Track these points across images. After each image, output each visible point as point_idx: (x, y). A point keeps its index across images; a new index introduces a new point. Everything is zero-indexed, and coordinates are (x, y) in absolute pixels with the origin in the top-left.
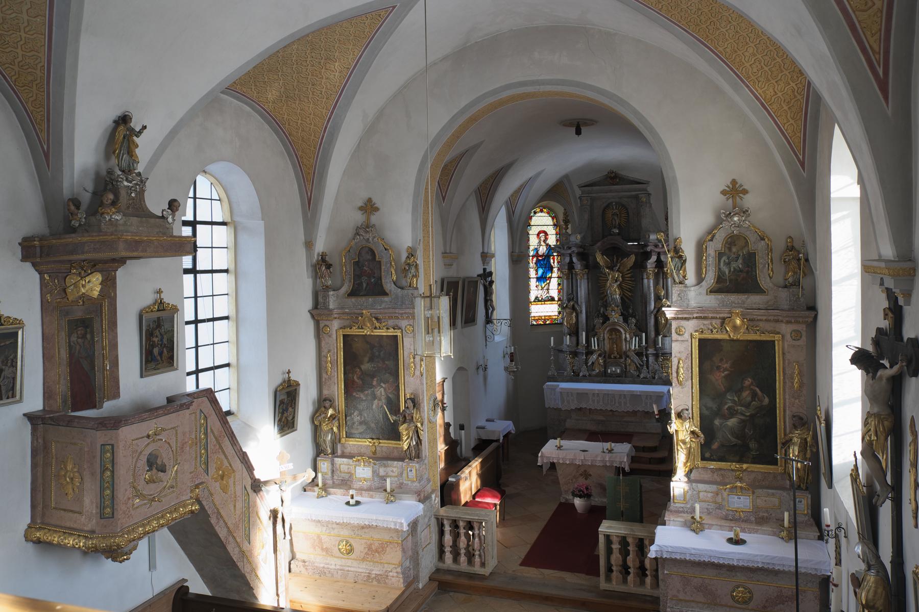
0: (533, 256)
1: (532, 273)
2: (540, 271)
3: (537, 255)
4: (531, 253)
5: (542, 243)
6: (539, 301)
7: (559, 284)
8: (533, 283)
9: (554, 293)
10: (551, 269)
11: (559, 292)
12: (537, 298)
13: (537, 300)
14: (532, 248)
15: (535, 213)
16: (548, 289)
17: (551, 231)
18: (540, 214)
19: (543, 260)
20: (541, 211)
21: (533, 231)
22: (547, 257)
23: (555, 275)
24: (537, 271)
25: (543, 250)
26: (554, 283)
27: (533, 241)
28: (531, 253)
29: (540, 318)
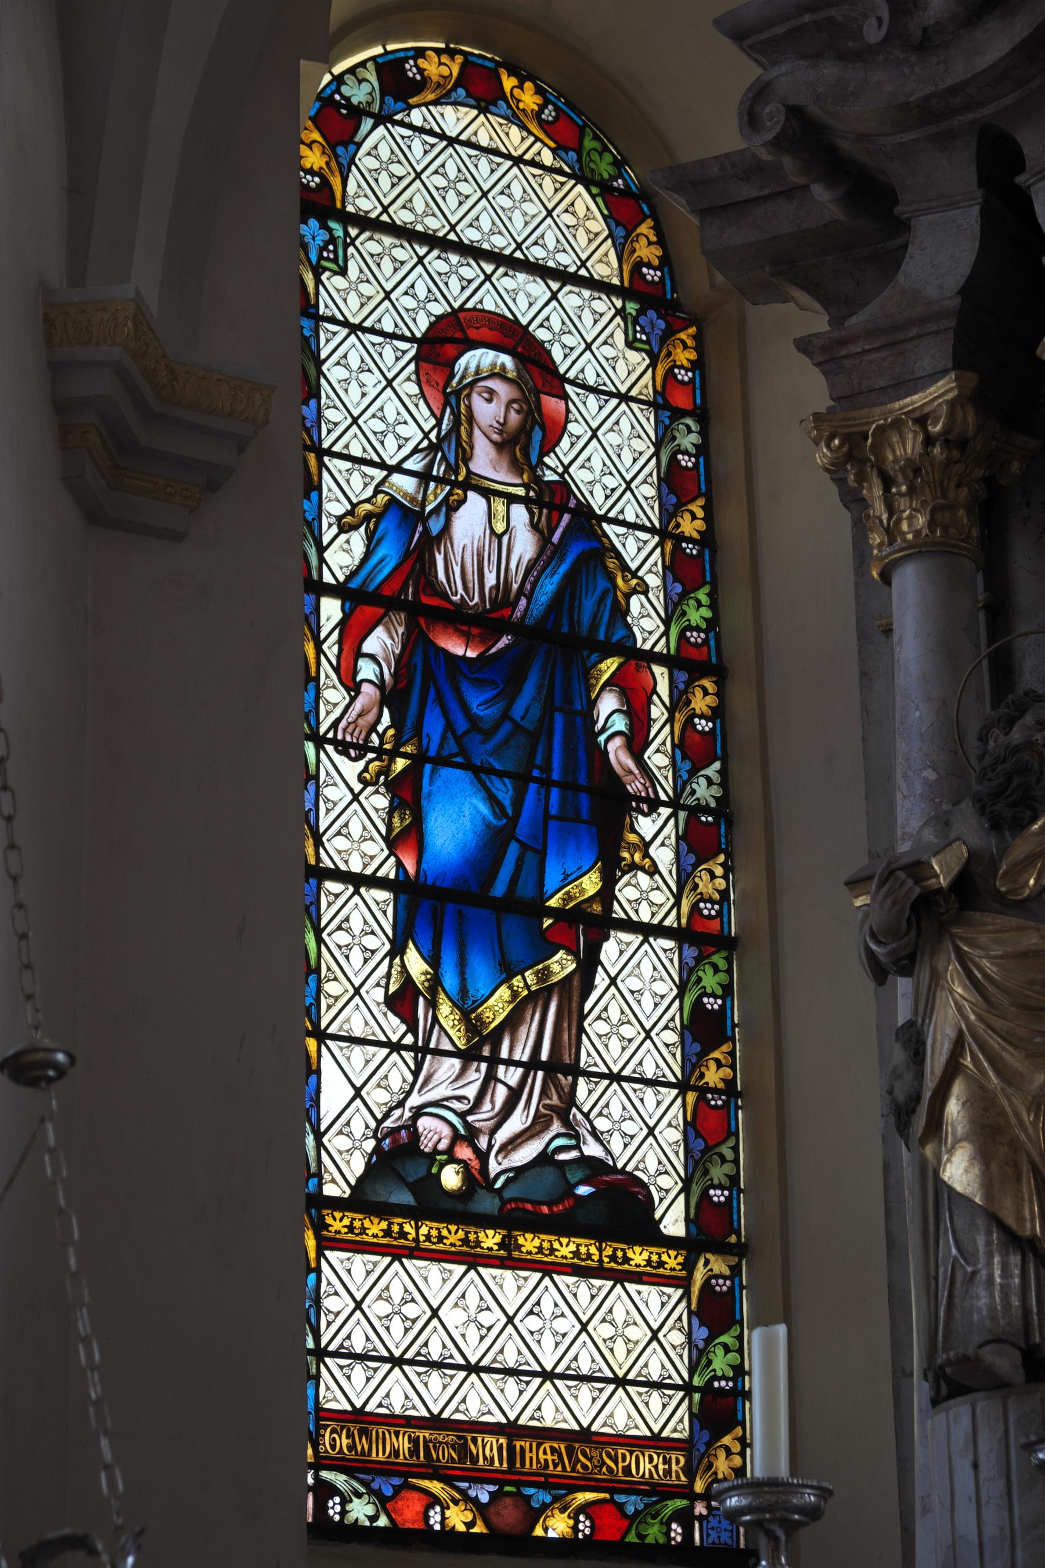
0: (363, 601)
1: (352, 822)
2: (455, 821)
3: (406, 589)
4: (343, 556)
5: (484, 461)
6: (432, 1204)
7: (702, 1030)
8: (356, 941)
9: (640, 1132)
10: (603, 814)
11: (705, 1136)
12: (398, 1154)
13: (410, 1192)
14: (343, 488)
15: (399, 85)
16: (561, 1068)
17: (592, 341)
18: (453, 119)
19: (501, 674)
20: (480, 90)
21: (374, 300)
22: (560, 625)
23: (642, 896)
24: (407, 796)
25: (486, 540)
26: (637, 991)
27: (371, 411)
28: (343, 556)
29: (445, 1447)
